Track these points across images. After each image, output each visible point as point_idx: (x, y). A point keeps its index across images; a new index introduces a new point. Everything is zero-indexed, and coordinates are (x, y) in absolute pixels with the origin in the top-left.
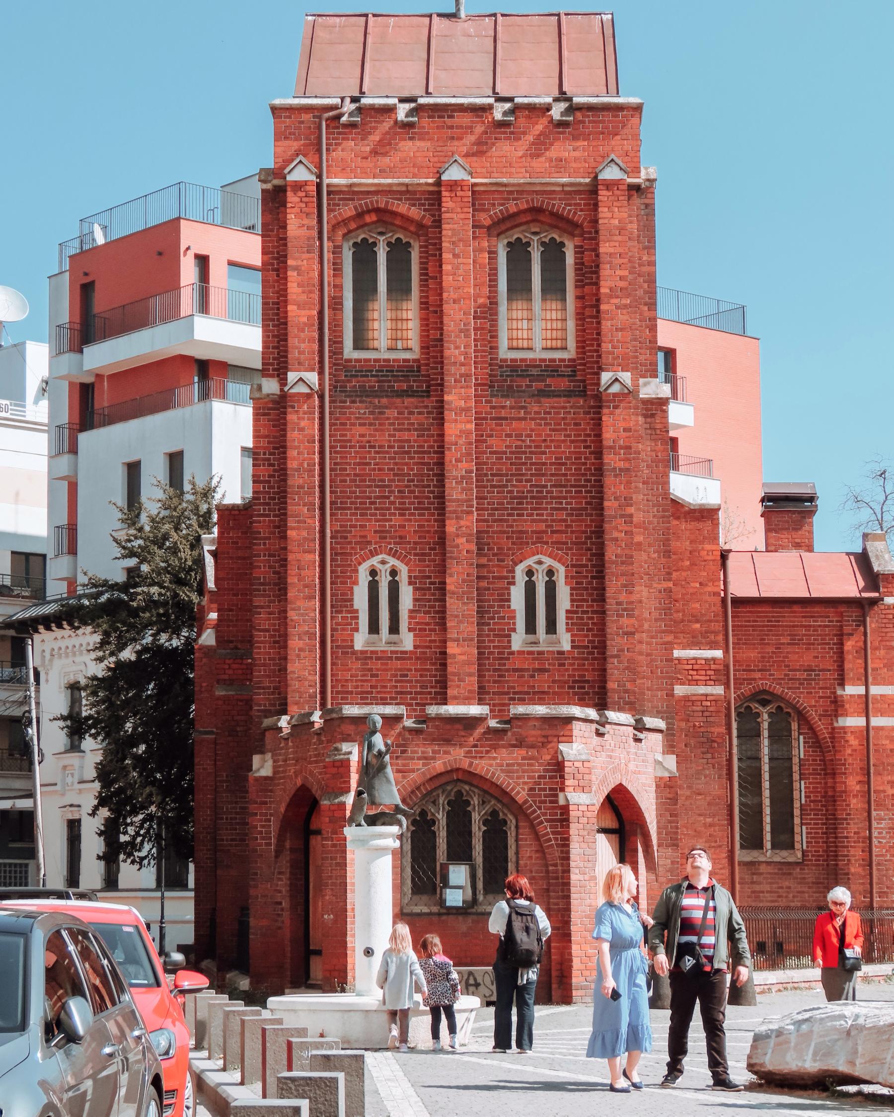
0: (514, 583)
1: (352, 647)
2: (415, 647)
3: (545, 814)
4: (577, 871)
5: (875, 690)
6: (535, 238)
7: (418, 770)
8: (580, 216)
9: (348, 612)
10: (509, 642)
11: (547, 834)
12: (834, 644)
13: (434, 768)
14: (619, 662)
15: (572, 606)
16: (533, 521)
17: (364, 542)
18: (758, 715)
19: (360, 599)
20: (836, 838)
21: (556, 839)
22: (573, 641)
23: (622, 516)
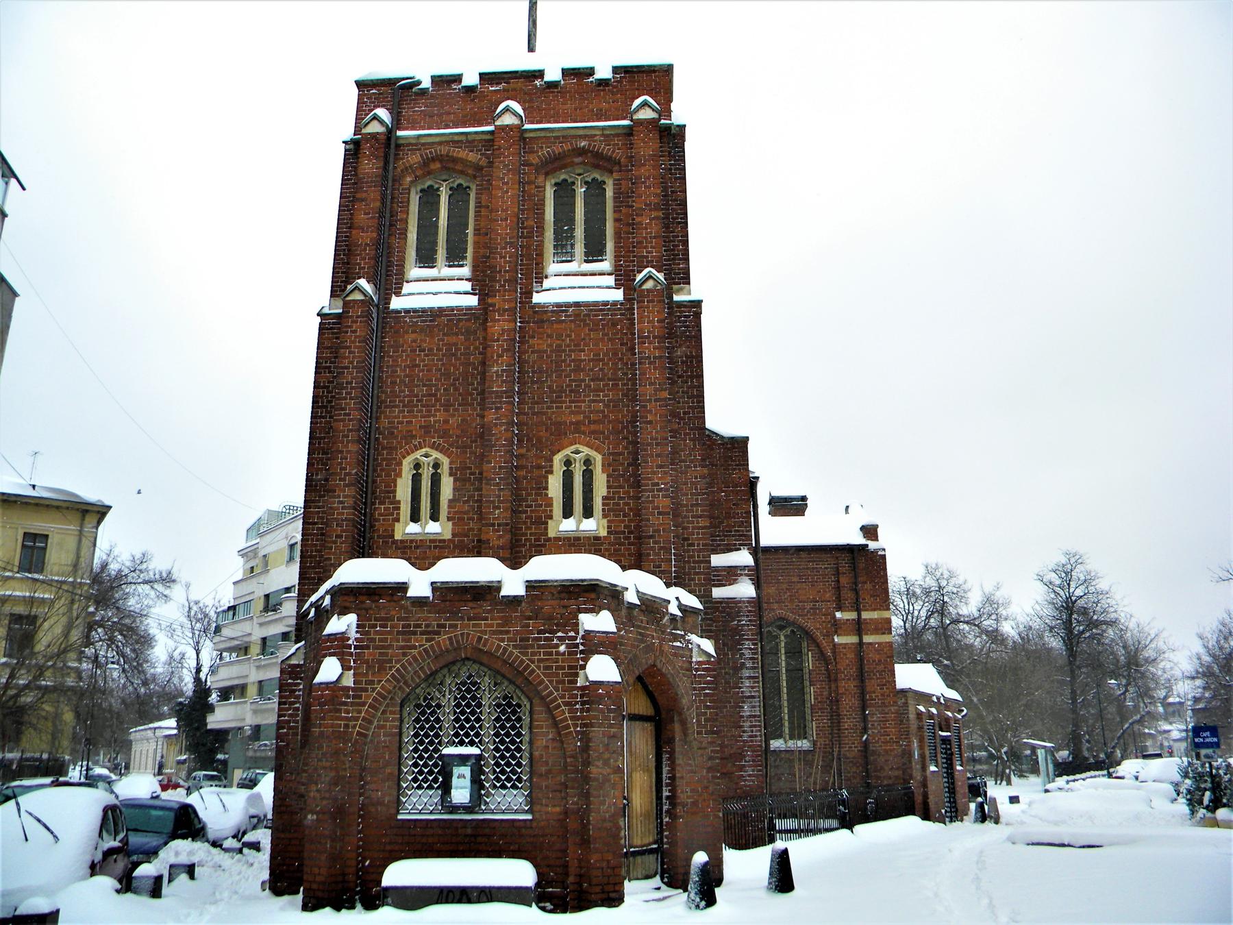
0: (552, 472)
1: (393, 536)
2: (454, 535)
3: (563, 697)
4: (600, 763)
5: (866, 615)
6: (579, 178)
7: (421, 646)
8: (618, 154)
9: (392, 503)
10: (546, 529)
11: (565, 719)
12: (832, 581)
13: (438, 644)
14: (655, 543)
15: (609, 492)
16: (572, 413)
17: (409, 436)
18: (777, 637)
19: (403, 491)
20: (839, 730)
21: (576, 726)
22: (609, 527)
23: (656, 400)
